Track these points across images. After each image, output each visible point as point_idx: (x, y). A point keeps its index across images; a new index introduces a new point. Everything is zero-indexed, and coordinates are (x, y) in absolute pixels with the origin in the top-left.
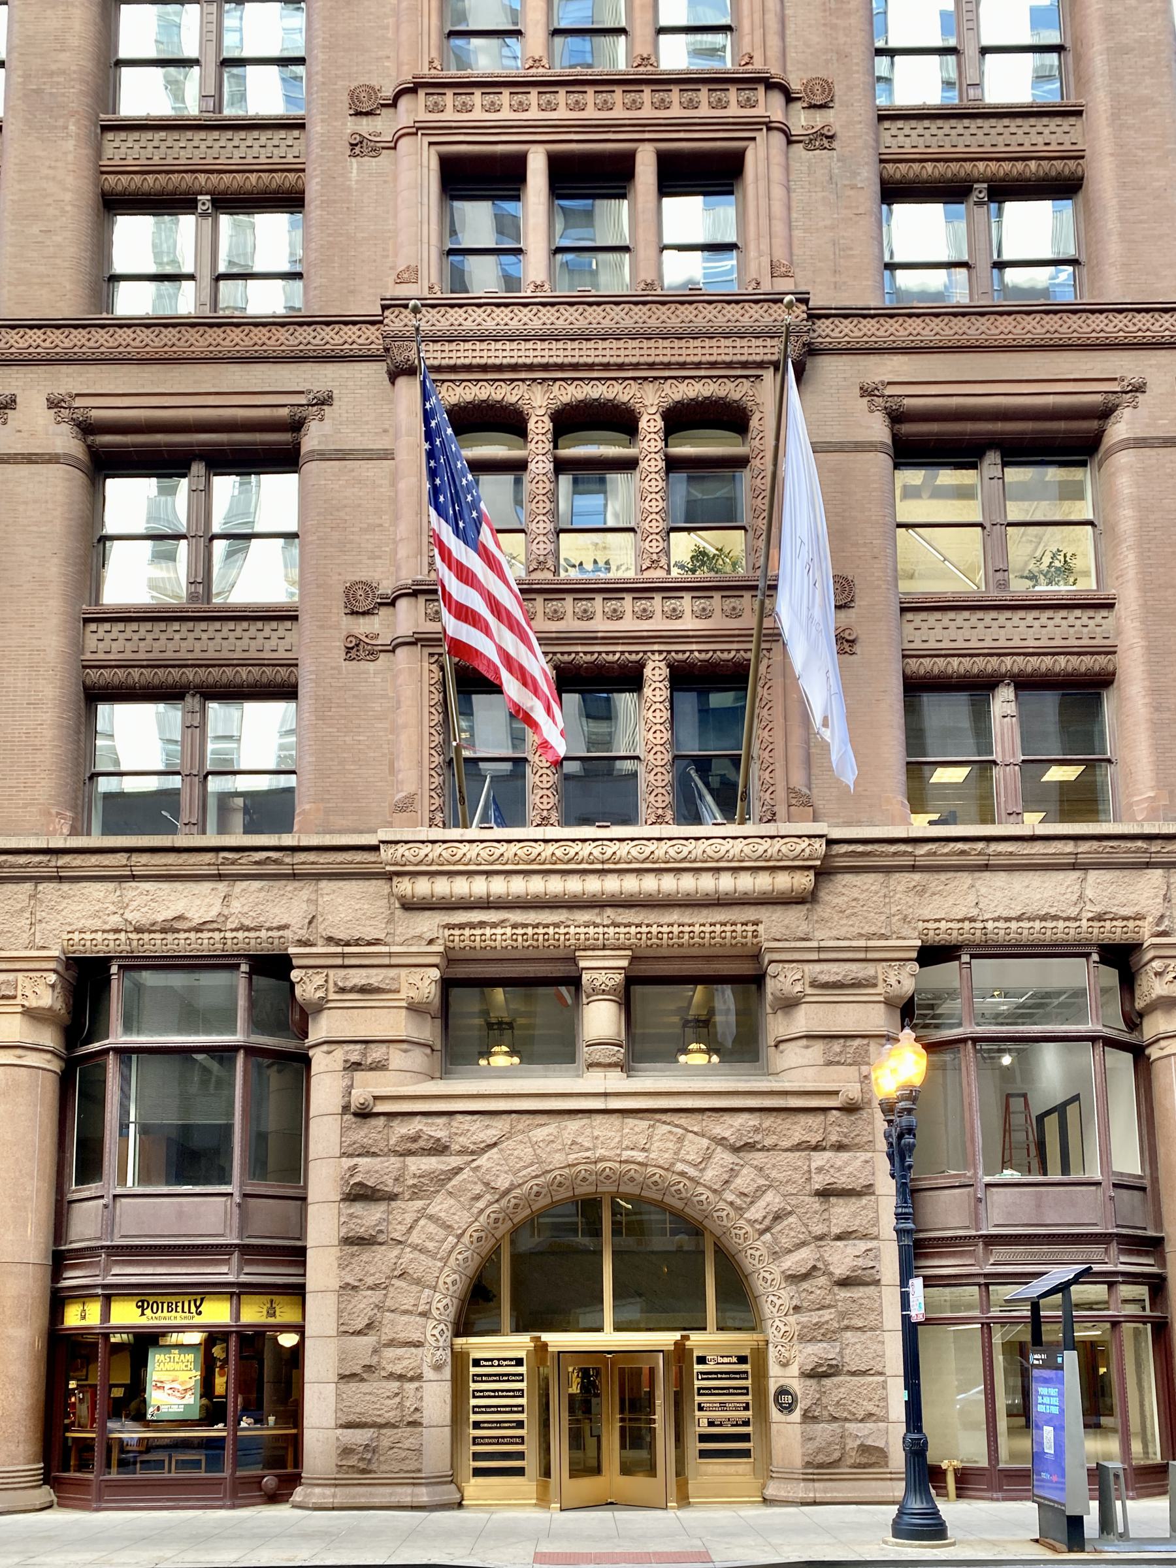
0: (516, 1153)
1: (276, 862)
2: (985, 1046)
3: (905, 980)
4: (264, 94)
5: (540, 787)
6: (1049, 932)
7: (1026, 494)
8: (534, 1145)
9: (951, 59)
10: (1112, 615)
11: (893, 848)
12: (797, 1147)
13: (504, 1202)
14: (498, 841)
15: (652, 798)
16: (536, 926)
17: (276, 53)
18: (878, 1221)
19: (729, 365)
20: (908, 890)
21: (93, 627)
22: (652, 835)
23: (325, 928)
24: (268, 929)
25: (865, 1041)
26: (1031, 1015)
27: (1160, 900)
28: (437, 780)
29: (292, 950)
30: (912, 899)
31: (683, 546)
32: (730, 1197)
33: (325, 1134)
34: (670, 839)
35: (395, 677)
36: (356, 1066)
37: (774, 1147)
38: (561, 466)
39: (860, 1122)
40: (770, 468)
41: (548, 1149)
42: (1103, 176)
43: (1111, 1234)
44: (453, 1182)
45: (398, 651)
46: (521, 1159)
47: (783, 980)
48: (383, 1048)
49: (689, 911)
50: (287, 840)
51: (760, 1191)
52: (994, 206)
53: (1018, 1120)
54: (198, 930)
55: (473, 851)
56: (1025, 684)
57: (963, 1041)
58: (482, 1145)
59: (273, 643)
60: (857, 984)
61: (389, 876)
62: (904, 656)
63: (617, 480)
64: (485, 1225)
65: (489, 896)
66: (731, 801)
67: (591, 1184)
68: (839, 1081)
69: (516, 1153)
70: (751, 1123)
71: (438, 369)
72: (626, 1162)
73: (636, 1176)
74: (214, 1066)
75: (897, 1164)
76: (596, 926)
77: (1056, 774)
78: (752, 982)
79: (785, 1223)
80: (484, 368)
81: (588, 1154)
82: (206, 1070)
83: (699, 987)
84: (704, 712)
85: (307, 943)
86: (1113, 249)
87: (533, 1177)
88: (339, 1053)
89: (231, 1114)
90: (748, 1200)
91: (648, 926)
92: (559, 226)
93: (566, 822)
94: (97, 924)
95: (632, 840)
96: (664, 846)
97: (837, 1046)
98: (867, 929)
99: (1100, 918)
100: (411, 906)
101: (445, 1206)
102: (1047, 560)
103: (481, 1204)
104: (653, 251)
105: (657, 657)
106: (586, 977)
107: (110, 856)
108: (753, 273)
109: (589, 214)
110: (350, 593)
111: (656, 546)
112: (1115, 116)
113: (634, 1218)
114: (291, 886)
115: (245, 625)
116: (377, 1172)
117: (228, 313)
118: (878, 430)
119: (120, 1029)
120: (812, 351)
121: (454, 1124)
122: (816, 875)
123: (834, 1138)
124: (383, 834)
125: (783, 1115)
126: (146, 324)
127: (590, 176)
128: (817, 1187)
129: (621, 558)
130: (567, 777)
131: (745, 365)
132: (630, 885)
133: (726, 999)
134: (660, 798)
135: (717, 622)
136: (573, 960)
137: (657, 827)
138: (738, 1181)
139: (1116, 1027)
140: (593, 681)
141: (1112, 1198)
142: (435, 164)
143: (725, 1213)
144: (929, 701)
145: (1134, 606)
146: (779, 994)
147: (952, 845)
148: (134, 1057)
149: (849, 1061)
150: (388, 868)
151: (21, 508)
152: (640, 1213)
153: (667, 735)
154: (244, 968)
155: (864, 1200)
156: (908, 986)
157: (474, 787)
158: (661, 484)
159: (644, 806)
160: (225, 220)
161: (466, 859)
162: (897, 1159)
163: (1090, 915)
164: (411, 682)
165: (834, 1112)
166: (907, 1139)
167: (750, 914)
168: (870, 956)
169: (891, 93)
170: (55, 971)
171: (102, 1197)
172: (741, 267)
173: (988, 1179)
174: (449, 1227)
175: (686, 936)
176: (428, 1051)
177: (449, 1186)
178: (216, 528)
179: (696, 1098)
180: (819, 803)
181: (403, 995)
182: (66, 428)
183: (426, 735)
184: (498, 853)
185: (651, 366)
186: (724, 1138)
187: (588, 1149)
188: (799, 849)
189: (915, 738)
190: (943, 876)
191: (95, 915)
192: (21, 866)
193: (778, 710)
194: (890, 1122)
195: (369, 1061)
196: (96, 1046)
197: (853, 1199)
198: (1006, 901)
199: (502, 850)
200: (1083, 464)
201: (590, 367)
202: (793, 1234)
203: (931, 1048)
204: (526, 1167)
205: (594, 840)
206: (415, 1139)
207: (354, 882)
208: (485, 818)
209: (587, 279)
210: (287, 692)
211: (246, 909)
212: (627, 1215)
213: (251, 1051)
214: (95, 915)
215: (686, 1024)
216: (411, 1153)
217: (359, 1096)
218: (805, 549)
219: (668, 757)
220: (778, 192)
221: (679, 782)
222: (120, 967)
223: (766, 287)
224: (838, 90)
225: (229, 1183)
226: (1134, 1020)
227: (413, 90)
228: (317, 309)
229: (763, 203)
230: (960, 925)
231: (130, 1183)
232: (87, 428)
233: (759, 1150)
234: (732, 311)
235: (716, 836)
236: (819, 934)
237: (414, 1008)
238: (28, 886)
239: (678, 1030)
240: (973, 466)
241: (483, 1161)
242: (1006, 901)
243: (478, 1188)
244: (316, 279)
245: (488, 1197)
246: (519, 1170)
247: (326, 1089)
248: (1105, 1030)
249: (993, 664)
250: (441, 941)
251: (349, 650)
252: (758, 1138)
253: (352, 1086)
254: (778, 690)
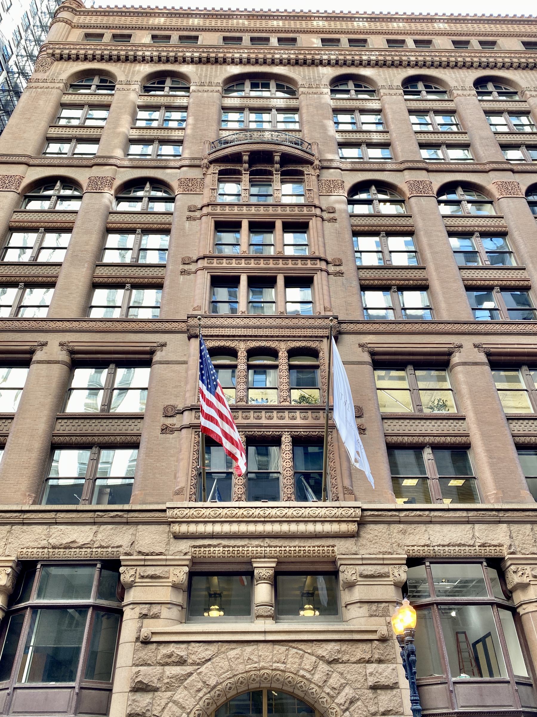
0: (220, 664)
1: (120, 517)
2: (443, 607)
3: (402, 574)
4: (152, 258)
5: (238, 485)
6: (462, 552)
7: (424, 379)
8: (229, 660)
9: (380, 254)
10: (465, 422)
11: (390, 513)
12: (359, 661)
13: (212, 693)
14: (219, 508)
15: (285, 490)
16: (234, 547)
17: (158, 248)
18: (402, 704)
19: (311, 337)
20: (399, 532)
21: (60, 421)
22: (286, 506)
23: (138, 547)
24: (113, 547)
25: (387, 604)
26: (461, 591)
27: (508, 538)
28: (194, 481)
29: (121, 558)
30: (401, 536)
31: (296, 394)
32: (328, 690)
33: (126, 652)
34: (294, 507)
35: (180, 440)
36: (144, 616)
37: (347, 662)
38: (249, 367)
39: (388, 647)
40: (327, 370)
41: (236, 662)
42: (435, 284)
43: (520, 711)
44: (188, 681)
45: (183, 430)
46: (222, 668)
47: (347, 574)
48: (159, 607)
49: (303, 540)
50: (126, 507)
51: (343, 686)
52: (399, 293)
53: (463, 646)
54: (80, 547)
55: (207, 512)
56: (435, 447)
57: (432, 604)
58: (203, 660)
59: (132, 427)
60: (380, 576)
61: (169, 523)
62: (385, 436)
63: (271, 372)
64: (202, 706)
65: (213, 532)
66: (319, 491)
67: (257, 682)
68: (377, 625)
69: (220, 664)
70: (336, 648)
71: (206, 336)
72: (275, 670)
73: (280, 678)
74: (77, 615)
75: (408, 671)
76: (261, 547)
77: (453, 483)
78: (332, 574)
79: (356, 705)
80: (223, 336)
81: (256, 665)
82: (72, 617)
83: (309, 577)
84: (306, 454)
86: (443, 305)
87: (228, 679)
88: (138, 609)
89: (81, 642)
90: (337, 691)
91: (285, 547)
92: (251, 294)
93: (249, 499)
94: (36, 544)
95: (277, 507)
96: (291, 510)
97: (374, 607)
99: (483, 545)
100: (178, 537)
101: (183, 695)
102: (436, 402)
103: (201, 694)
104: (283, 303)
105: (286, 433)
106: (256, 571)
107: (48, 514)
108: (318, 309)
109: (261, 293)
110: (166, 409)
111: (286, 394)
112: (436, 269)
113: (279, 701)
114: (126, 527)
115: (122, 420)
116: (149, 675)
117: (131, 317)
118: (367, 358)
119: (35, 596)
120: (340, 333)
121: (190, 648)
122: (359, 524)
123: (376, 656)
124: (169, 505)
125: (351, 644)
126: (101, 320)
127: (260, 282)
128: (370, 684)
129: (272, 398)
130: (250, 479)
131: (316, 337)
132: (277, 528)
133: (321, 581)
134: (289, 490)
135: (310, 421)
136: (251, 563)
137: (288, 502)
138: (331, 681)
139: (501, 599)
140: (261, 443)
141: (517, 690)
142: (209, 278)
143: (325, 699)
144: (397, 452)
145: (473, 419)
146: (345, 580)
147: (415, 512)
148: (39, 610)
149: (380, 614)
150: (169, 520)
151: (41, 378)
152: (281, 699)
153: (291, 464)
154: (99, 566)
155: (395, 692)
156: (404, 577)
157: (210, 484)
158: (287, 374)
159: (282, 493)
160: (134, 292)
161: (204, 516)
162: (408, 668)
163: (479, 544)
164: (186, 443)
165: (376, 642)
166: (412, 658)
167: (330, 542)
168: (385, 562)
169: (361, 262)
170: (11, 567)
171: (8, 689)
172: (314, 308)
173: (454, 679)
174: (184, 707)
175: (302, 552)
176: (180, 608)
177: (185, 683)
178: (116, 386)
179: (309, 634)
180: (356, 493)
181: (170, 580)
182: (64, 352)
183: (191, 463)
184: (218, 513)
185: (283, 336)
186: (323, 656)
187: (256, 663)
188: (350, 513)
189: (394, 467)
190: (413, 526)
191: (36, 541)
192: (7, 518)
193: (336, 455)
194: (402, 647)
195: (151, 613)
196: (22, 605)
197: (389, 691)
198: (442, 538)
199: (220, 511)
200: (444, 370)
201: (261, 336)
202: (360, 712)
203: (418, 608)
204: (224, 673)
205: (261, 508)
206: (170, 656)
207: (153, 526)
208: (213, 498)
209: (260, 311)
210: (135, 446)
211: (104, 538)
212: (275, 700)
213: (96, 608)
214: (36, 541)
215: (303, 595)
216: (167, 664)
217: (145, 632)
218: (343, 397)
219: (292, 472)
220: (325, 288)
221: (297, 483)
222: (42, 565)
223: (323, 314)
224: (343, 261)
225: (73, 680)
226: (508, 594)
227: (203, 258)
228: (164, 317)
229: (321, 291)
230: (423, 548)
231: (23, 681)
232: (72, 352)
233: (341, 663)
234: (311, 321)
235: (313, 506)
236: (362, 552)
237: (175, 587)
238: (8, 527)
239: (299, 598)
240: (403, 370)
241: (203, 669)
242: (442, 538)
243: (200, 685)
244: (165, 309)
245: (205, 690)
246: (221, 674)
247: (129, 629)
248: (496, 599)
249: (421, 439)
250: (190, 554)
251: (162, 430)
252: (340, 656)
253: (142, 627)
254: (336, 447)
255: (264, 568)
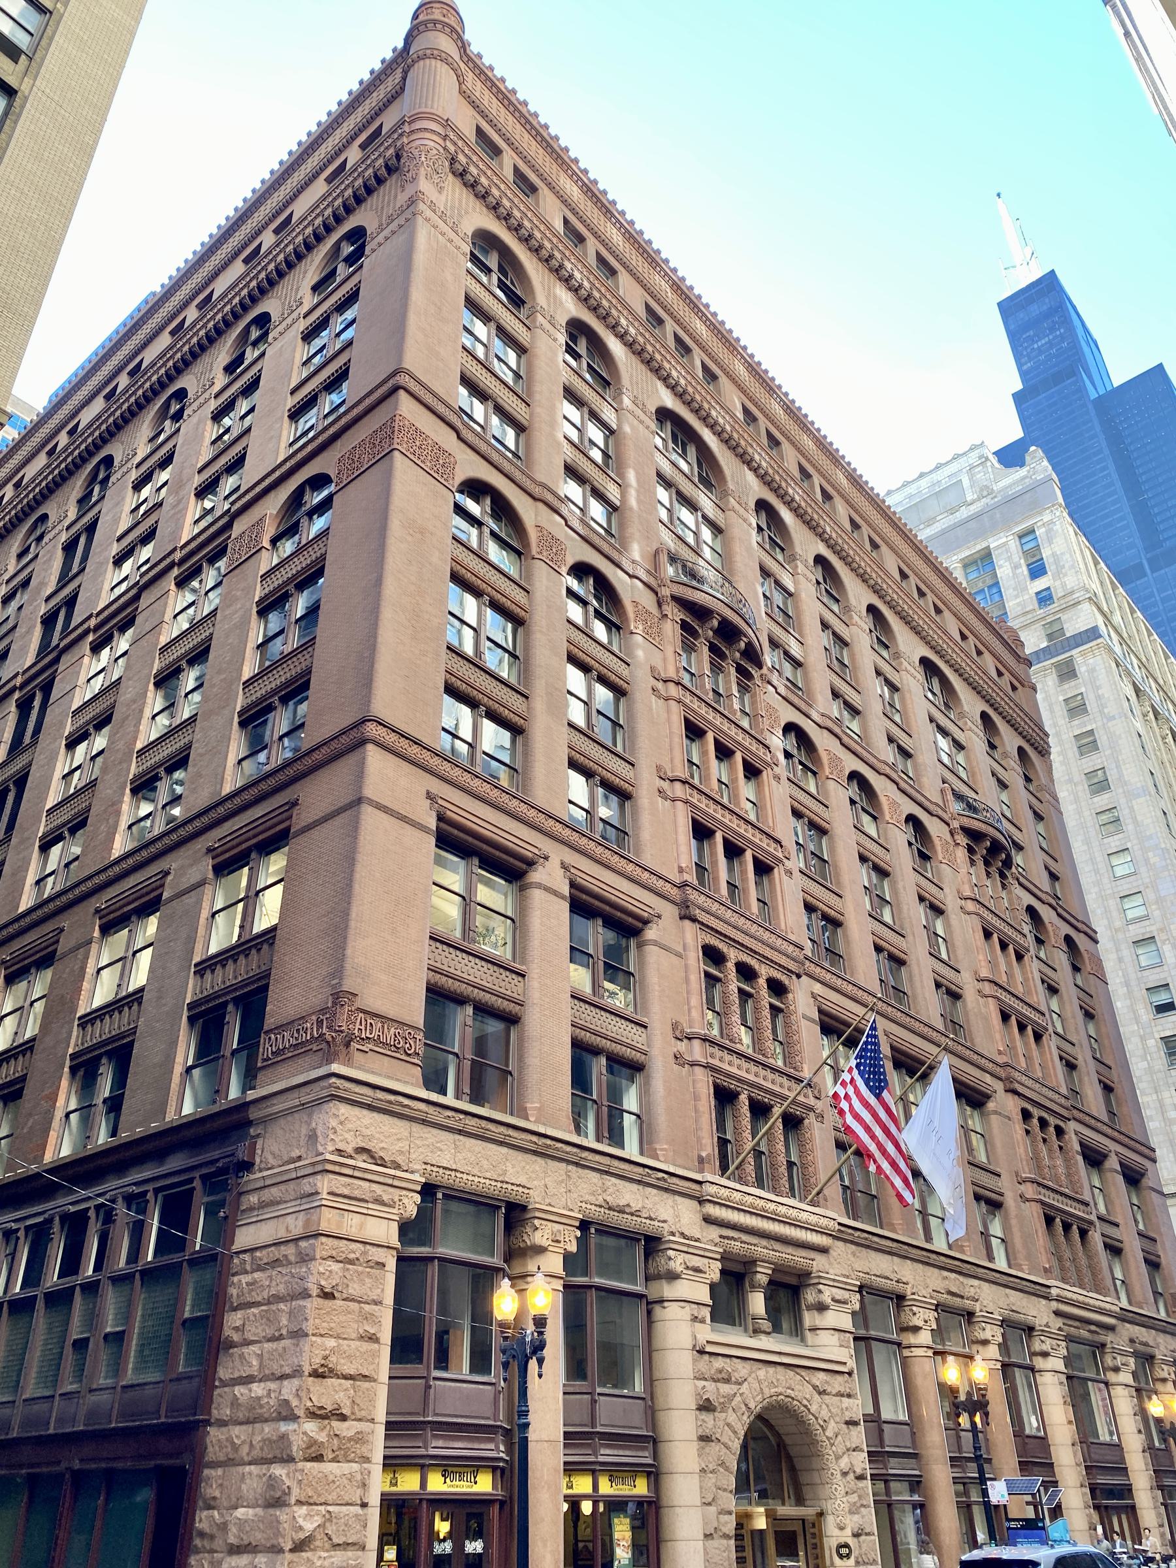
85: (673, 1234)
94: (592, 1199)
98: (844, 1272)
100: (708, 1220)
114: (666, 1195)
167: (812, 1254)
206: (720, 1372)
255: (763, 1275)
